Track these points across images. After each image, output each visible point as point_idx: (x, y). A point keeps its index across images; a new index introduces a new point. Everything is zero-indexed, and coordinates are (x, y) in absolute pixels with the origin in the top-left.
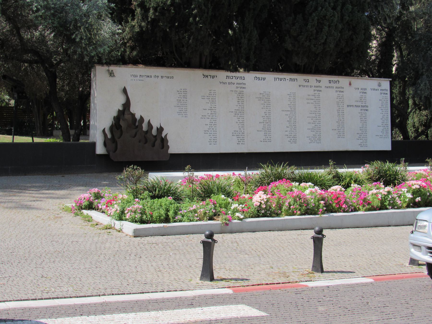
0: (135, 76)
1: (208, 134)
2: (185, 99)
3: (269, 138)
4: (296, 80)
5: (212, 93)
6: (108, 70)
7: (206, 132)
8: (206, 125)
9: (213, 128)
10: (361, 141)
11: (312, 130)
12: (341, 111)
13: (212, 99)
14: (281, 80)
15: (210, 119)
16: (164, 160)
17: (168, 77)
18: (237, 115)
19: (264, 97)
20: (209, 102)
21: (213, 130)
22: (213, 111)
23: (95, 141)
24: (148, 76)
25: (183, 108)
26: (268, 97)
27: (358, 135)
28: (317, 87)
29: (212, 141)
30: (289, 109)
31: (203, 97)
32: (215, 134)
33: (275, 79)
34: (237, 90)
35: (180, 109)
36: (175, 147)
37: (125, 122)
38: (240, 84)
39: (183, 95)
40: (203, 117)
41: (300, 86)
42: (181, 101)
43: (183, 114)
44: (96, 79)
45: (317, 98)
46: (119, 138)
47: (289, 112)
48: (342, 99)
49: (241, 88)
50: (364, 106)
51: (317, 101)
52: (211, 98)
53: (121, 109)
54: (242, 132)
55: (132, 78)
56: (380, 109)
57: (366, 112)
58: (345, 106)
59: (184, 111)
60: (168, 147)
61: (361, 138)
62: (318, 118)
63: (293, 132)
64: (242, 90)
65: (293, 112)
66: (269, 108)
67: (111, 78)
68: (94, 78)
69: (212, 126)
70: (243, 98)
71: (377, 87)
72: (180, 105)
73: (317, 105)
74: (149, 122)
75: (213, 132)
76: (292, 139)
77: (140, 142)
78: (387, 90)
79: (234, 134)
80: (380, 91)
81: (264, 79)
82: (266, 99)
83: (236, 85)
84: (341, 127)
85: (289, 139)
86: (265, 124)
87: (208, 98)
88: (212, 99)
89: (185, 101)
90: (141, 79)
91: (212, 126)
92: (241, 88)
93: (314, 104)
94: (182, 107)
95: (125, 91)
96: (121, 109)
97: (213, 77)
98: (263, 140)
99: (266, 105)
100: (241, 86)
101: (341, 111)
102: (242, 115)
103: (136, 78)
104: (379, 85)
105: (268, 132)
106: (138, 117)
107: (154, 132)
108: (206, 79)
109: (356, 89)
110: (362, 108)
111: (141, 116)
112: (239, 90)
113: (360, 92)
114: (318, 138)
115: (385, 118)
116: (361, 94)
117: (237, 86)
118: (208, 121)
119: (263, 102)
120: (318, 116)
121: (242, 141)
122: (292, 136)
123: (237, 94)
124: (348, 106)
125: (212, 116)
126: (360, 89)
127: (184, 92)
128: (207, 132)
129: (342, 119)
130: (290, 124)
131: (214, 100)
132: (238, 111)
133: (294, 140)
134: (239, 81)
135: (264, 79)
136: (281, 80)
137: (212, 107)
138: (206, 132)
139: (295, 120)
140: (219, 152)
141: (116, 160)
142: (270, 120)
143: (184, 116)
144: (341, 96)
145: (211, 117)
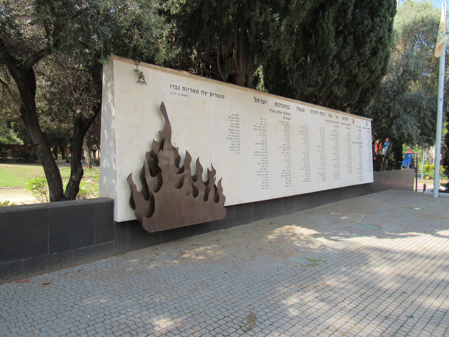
1: (261, 176)
2: (237, 129)
6: (136, 71)
8: (258, 164)
9: (265, 168)
14: (315, 112)
16: (220, 218)
17: (218, 96)
21: (265, 171)
22: (264, 145)
23: (111, 196)
24: (194, 91)
36: (232, 197)
37: (160, 163)
39: (235, 122)
42: (234, 131)
43: (236, 149)
44: (113, 85)
46: (157, 190)
53: (157, 140)
55: (172, 90)
60: (224, 198)
67: (139, 85)
68: (109, 84)
72: (232, 137)
77: (188, 195)
79: (283, 174)
81: (303, 110)
86: (305, 161)
89: (237, 132)
90: (184, 93)
94: (234, 140)
95: (162, 109)
96: (157, 140)
98: (304, 180)
103: (177, 91)
106: (182, 153)
107: (204, 178)
111: (187, 153)
127: (235, 118)
128: (259, 173)
136: (315, 112)
140: (270, 199)
141: (153, 231)
143: (237, 152)
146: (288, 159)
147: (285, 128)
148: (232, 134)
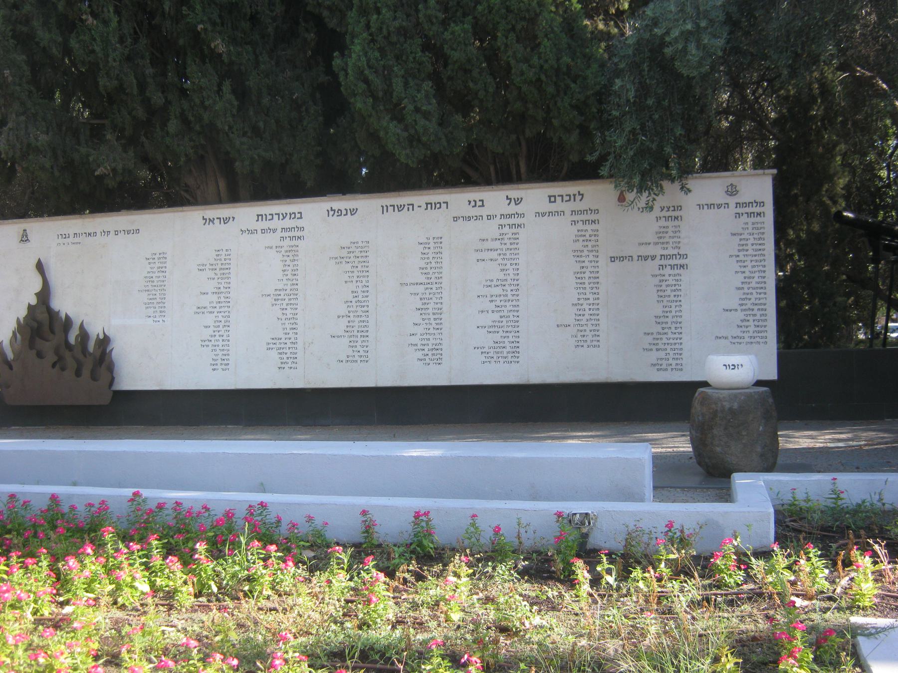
0: (66, 236)
1: (210, 348)
2: (161, 274)
3: (362, 353)
4: (444, 206)
5: (223, 257)
7: (204, 343)
9: (220, 333)
10: (662, 354)
11: (490, 330)
12: (587, 275)
13: (221, 269)
15: (216, 314)
17: (129, 232)
18: (279, 302)
19: (352, 255)
20: (213, 276)
21: (221, 339)
22: (222, 295)
25: (158, 293)
26: (364, 254)
27: (649, 339)
28: (510, 216)
29: (219, 362)
30: (422, 279)
31: (201, 267)
32: (226, 348)
33: (385, 209)
34: (282, 243)
35: (151, 297)
38: (290, 229)
39: (158, 265)
41: (456, 219)
42: (154, 279)
45: (508, 246)
47: (422, 287)
48: (593, 243)
49: (291, 238)
50: (671, 257)
51: (508, 252)
52: (218, 267)
54: (293, 340)
55: (61, 241)
57: (681, 271)
58: (603, 261)
59: (159, 300)
61: (661, 346)
62: (510, 297)
63: (431, 337)
64: (294, 242)
65: (434, 286)
66: (364, 280)
69: (221, 328)
70: (296, 263)
71: (721, 198)
72: (150, 288)
73: (508, 263)
74: (82, 326)
75: (221, 343)
76: (430, 353)
78: (762, 204)
79: (271, 346)
80: (732, 209)
81: (353, 212)
82: (357, 260)
83: (279, 234)
85: (419, 354)
86: (352, 319)
87: (214, 267)
88: (221, 269)
89: (161, 279)
90: (77, 240)
91: (221, 328)
92: (291, 238)
93: (500, 261)
94: (154, 292)
95: (40, 267)
96: (34, 301)
97: (226, 221)
99: (356, 274)
100: (291, 234)
101: (587, 275)
102: (292, 302)
104: (732, 191)
105: (360, 339)
112: (287, 242)
113: (658, 219)
114: (508, 349)
115: (753, 285)
116: (662, 223)
117: (663, 262)
118: (209, 320)
119: (348, 267)
120: (509, 293)
121: (290, 361)
122: (430, 347)
123: (283, 253)
124: (613, 259)
125: (221, 307)
127: (159, 258)
128: (207, 343)
129: (591, 297)
130: (424, 317)
131: (227, 271)
132: (282, 293)
133: (435, 355)
134: (288, 223)
135: (353, 212)
136: (400, 208)
137: (221, 286)
138: (204, 343)
139: (439, 306)
143: (158, 310)
145: (218, 309)
146: (289, 316)
147: (286, 258)
148: (150, 284)
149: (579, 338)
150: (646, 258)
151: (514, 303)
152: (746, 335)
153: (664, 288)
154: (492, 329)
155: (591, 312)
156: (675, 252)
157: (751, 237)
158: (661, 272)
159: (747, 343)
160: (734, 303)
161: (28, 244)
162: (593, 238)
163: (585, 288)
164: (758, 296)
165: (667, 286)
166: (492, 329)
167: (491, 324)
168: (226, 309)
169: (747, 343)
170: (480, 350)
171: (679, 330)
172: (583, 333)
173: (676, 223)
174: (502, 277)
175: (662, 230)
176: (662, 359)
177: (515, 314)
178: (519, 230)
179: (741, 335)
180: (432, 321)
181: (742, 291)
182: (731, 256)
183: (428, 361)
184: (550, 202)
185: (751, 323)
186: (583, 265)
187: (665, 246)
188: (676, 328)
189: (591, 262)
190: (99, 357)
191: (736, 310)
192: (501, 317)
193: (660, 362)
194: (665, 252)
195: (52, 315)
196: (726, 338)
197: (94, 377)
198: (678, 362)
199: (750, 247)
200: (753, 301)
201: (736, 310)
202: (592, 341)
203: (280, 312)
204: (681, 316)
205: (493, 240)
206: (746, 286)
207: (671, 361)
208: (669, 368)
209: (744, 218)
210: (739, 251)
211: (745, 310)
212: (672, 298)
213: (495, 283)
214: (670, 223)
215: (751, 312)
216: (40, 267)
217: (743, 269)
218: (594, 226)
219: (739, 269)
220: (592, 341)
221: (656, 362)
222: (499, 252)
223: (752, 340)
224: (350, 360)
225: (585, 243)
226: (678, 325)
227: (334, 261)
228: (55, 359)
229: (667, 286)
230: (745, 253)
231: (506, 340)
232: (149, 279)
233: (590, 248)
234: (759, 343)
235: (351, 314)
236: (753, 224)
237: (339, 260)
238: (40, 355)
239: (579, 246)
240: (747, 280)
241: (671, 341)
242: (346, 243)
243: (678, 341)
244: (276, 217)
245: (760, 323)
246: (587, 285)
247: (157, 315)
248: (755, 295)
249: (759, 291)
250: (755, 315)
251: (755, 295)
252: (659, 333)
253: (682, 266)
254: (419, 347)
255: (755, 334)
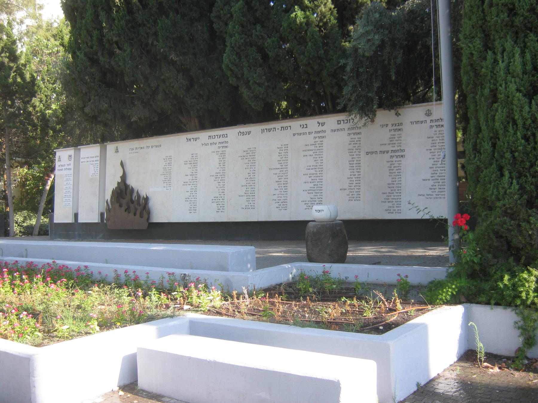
0: (132, 149)
1: (189, 202)
2: (169, 166)
3: (252, 204)
4: (289, 128)
10: (390, 204)
11: (309, 192)
12: (355, 162)
19: (248, 155)
20: (190, 167)
26: (253, 154)
27: (385, 196)
28: (319, 132)
30: (279, 166)
33: (263, 131)
40: (185, 184)
41: (294, 135)
45: (318, 148)
47: (279, 170)
48: (358, 145)
51: (318, 151)
53: (120, 181)
55: (131, 151)
56: (429, 151)
57: (401, 159)
58: (363, 154)
61: (390, 200)
62: (318, 175)
63: (282, 196)
64: (224, 149)
65: (284, 170)
66: (253, 167)
71: (422, 117)
73: (318, 157)
76: (282, 204)
79: (214, 201)
80: (429, 124)
81: (249, 133)
82: (250, 157)
83: (218, 145)
84: (354, 184)
85: (277, 205)
86: (248, 187)
90: (137, 151)
93: (314, 156)
96: (120, 180)
97: (196, 139)
98: (244, 207)
101: (355, 162)
103: (133, 151)
104: (429, 113)
105: (251, 197)
108: (189, 143)
109: (383, 126)
110: (393, 154)
112: (221, 149)
113: (390, 130)
115: (439, 165)
116: (393, 133)
118: (188, 188)
119: (246, 161)
120: (318, 172)
121: (221, 208)
124: (367, 153)
126: (390, 126)
129: (357, 174)
132: (218, 174)
133: (283, 205)
134: (222, 140)
135: (249, 133)
136: (270, 130)
139: (286, 180)
142: (253, 182)
144: (357, 139)
145: (192, 183)
146: (222, 186)
149: (351, 196)
150: (384, 152)
151: (320, 178)
152: (434, 194)
153: (392, 168)
154: (309, 191)
155: (357, 182)
156: (399, 148)
157: (438, 139)
158: (391, 160)
159: (435, 198)
160: (428, 176)
161: (118, 154)
162: (358, 142)
163: (353, 169)
164: (441, 172)
165: (394, 167)
166: (309, 191)
167: (309, 189)
168: (195, 183)
169: (435, 198)
170: (304, 203)
171: (400, 191)
172: (352, 193)
173: (399, 132)
174: (315, 164)
175: (392, 136)
176: (391, 207)
177: (321, 183)
178: (323, 139)
179: (431, 193)
180: (283, 188)
181: (432, 169)
182: (427, 150)
183: (281, 208)
184: (338, 124)
185: (437, 187)
186: (353, 157)
187: (393, 145)
188: (398, 190)
189: (357, 155)
190: (142, 206)
191: (429, 180)
192: (314, 185)
193: (390, 209)
194: (394, 149)
195: (126, 186)
196: (424, 195)
197: (141, 216)
198: (399, 208)
199: (437, 144)
200: (438, 174)
201: (429, 180)
202: (357, 197)
203: (218, 184)
204: (401, 184)
205: (311, 145)
206: (434, 166)
207: (395, 208)
208: (394, 212)
209: (435, 128)
210: (432, 147)
211: (434, 180)
212: (397, 174)
213: (311, 167)
214: (396, 133)
215: (437, 181)
216: (122, 164)
217: (433, 157)
218: (359, 136)
219: (431, 157)
220: (357, 197)
221: (387, 209)
222: (314, 151)
223: (438, 197)
224: (247, 208)
225: (354, 145)
226: (399, 188)
227: (241, 158)
228: (126, 207)
229: (394, 167)
230: (434, 148)
231: (316, 197)
232: (165, 169)
233: (357, 148)
234: (441, 198)
235: (248, 185)
236: (439, 131)
237: (243, 157)
238: (121, 206)
239: (351, 147)
240: (435, 163)
241: (396, 197)
242: (246, 149)
243: (399, 197)
244: (216, 137)
245: (442, 187)
246: (355, 168)
247: (168, 186)
248: (439, 171)
249: (441, 169)
250: (439, 182)
251: (439, 171)
252: (390, 193)
253: (402, 156)
254: (277, 201)
255: (439, 193)
